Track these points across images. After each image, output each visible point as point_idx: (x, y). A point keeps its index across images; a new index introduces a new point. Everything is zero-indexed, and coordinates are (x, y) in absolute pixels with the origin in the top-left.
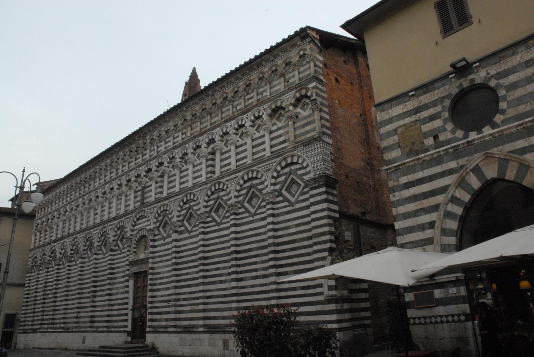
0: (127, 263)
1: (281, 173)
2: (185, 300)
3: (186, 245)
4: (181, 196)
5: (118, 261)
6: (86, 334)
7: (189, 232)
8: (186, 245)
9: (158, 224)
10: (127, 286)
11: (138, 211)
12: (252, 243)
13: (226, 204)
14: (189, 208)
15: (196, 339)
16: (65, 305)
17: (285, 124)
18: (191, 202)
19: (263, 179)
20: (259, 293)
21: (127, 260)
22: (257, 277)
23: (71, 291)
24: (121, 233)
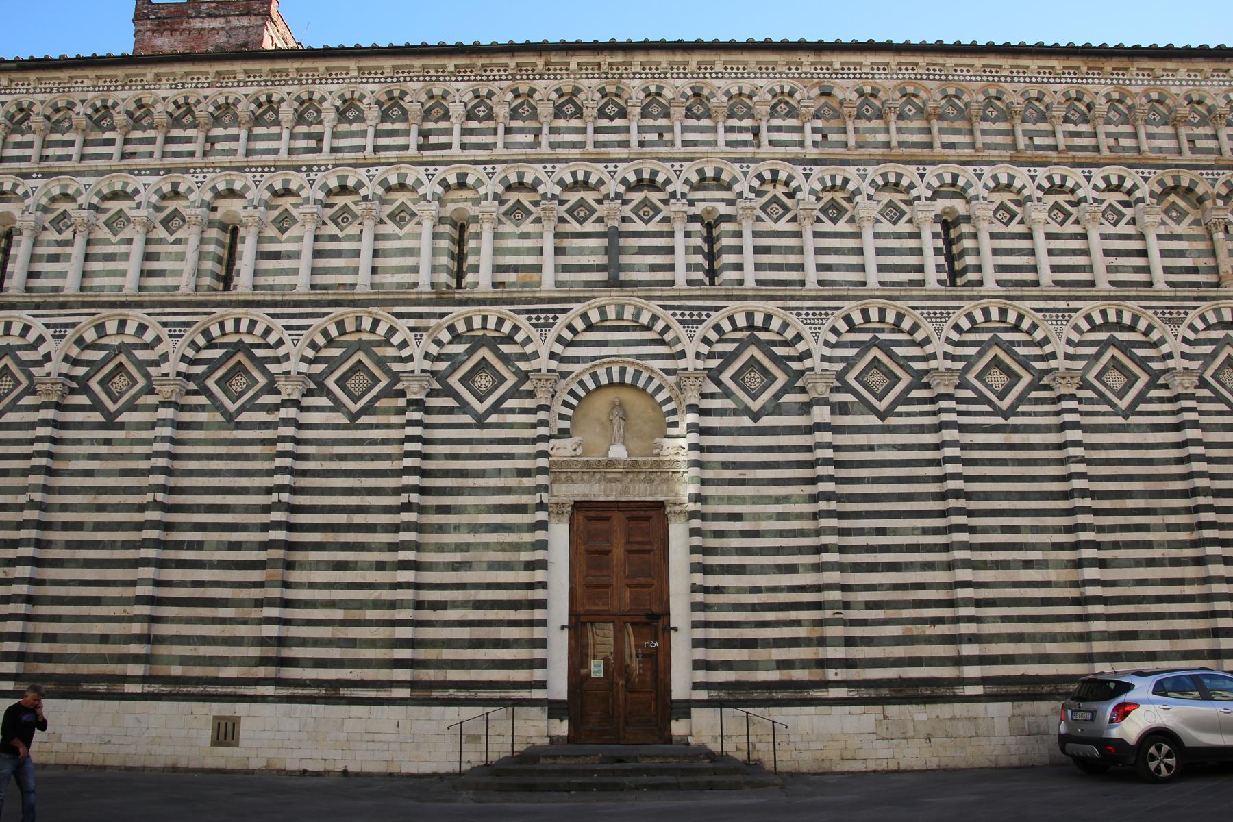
0: (542, 462)
1: (1202, 336)
2: (870, 605)
3: (871, 448)
4: (846, 305)
5: (465, 449)
6: (241, 709)
7: (882, 416)
8: (871, 448)
9: (714, 363)
10: (543, 545)
11: (600, 301)
12: (1130, 478)
13: (1027, 367)
14: (864, 347)
15: (953, 718)
16: (32, 581)
17: (1191, 232)
18: (882, 331)
19: (1155, 336)
20: (1159, 599)
21: (545, 454)
22: (1151, 562)
23: (78, 526)
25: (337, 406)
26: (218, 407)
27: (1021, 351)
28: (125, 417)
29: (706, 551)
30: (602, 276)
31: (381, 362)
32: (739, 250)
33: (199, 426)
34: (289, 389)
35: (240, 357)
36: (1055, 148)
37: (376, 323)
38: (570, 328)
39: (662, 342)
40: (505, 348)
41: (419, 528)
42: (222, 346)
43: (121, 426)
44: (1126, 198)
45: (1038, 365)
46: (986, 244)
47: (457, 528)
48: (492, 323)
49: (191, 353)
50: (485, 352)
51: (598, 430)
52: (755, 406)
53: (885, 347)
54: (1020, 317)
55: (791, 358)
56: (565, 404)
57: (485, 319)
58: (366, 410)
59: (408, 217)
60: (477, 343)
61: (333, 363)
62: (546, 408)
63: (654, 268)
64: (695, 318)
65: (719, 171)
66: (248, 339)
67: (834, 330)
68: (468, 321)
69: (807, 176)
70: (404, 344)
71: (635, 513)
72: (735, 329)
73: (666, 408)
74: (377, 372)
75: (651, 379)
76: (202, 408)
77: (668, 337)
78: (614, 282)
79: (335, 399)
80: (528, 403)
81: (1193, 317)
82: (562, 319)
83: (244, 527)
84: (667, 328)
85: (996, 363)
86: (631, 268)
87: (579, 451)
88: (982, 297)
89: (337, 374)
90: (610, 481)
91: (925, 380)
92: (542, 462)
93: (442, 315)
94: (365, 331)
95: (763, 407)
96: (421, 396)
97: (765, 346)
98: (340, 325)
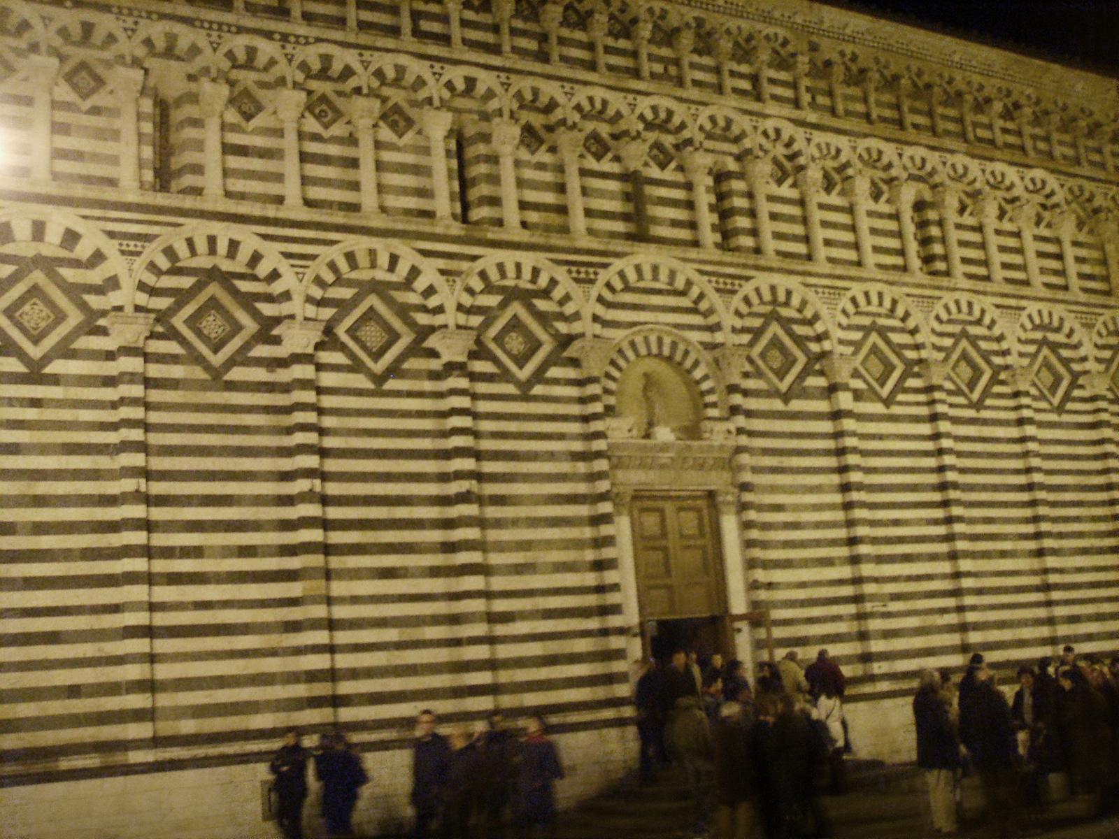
0: (599, 445)
3: (880, 437)
5: (512, 426)
7: (888, 402)
8: (880, 437)
13: (988, 362)
14: (867, 330)
18: (879, 315)
24: (503, 305)
25: (356, 367)
26: (198, 359)
27: (984, 345)
28: (57, 367)
29: (764, 545)
30: (620, 226)
31: (403, 311)
32: (752, 213)
33: (173, 384)
34: (297, 339)
35: (214, 289)
36: (992, 142)
37: (394, 260)
38: (609, 286)
39: (694, 311)
40: (541, 305)
41: (482, 523)
42: (350, 283)
43: (55, 380)
44: (1043, 201)
45: (998, 360)
46: (954, 235)
47: (515, 522)
48: (527, 273)
49: (151, 279)
50: (516, 308)
52: (784, 386)
53: (883, 332)
54: (983, 312)
55: (808, 338)
57: (518, 266)
58: (394, 371)
59: (402, 124)
60: (511, 295)
61: (344, 307)
62: (593, 380)
63: (675, 223)
64: (729, 287)
65: (729, 122)
66: (226, 266)
67: (844, 312)
68: (501, 268)
69: (809, 140)
70: (430, 291)
72: (762, 302)
74: (397, 324)
75: (686, 353)
76: (173, 359)
77: (703, 306)
78: (640, 236)
79: (352, 355)
80: (571, 373)
81: (1099, 326)
82: (603, 276)
83: (255, 526)
84: (702, 296)
85: (964, 356)
86: (655, 221)
88: (955, 289)
89: (348, 322)
91: (916, 369)
92: (599, 445)
93: (474, 258)
94: (381, 268)
95: (789, 389)
96: (462, 358)
97: (786, 323)
98: (350, 257)
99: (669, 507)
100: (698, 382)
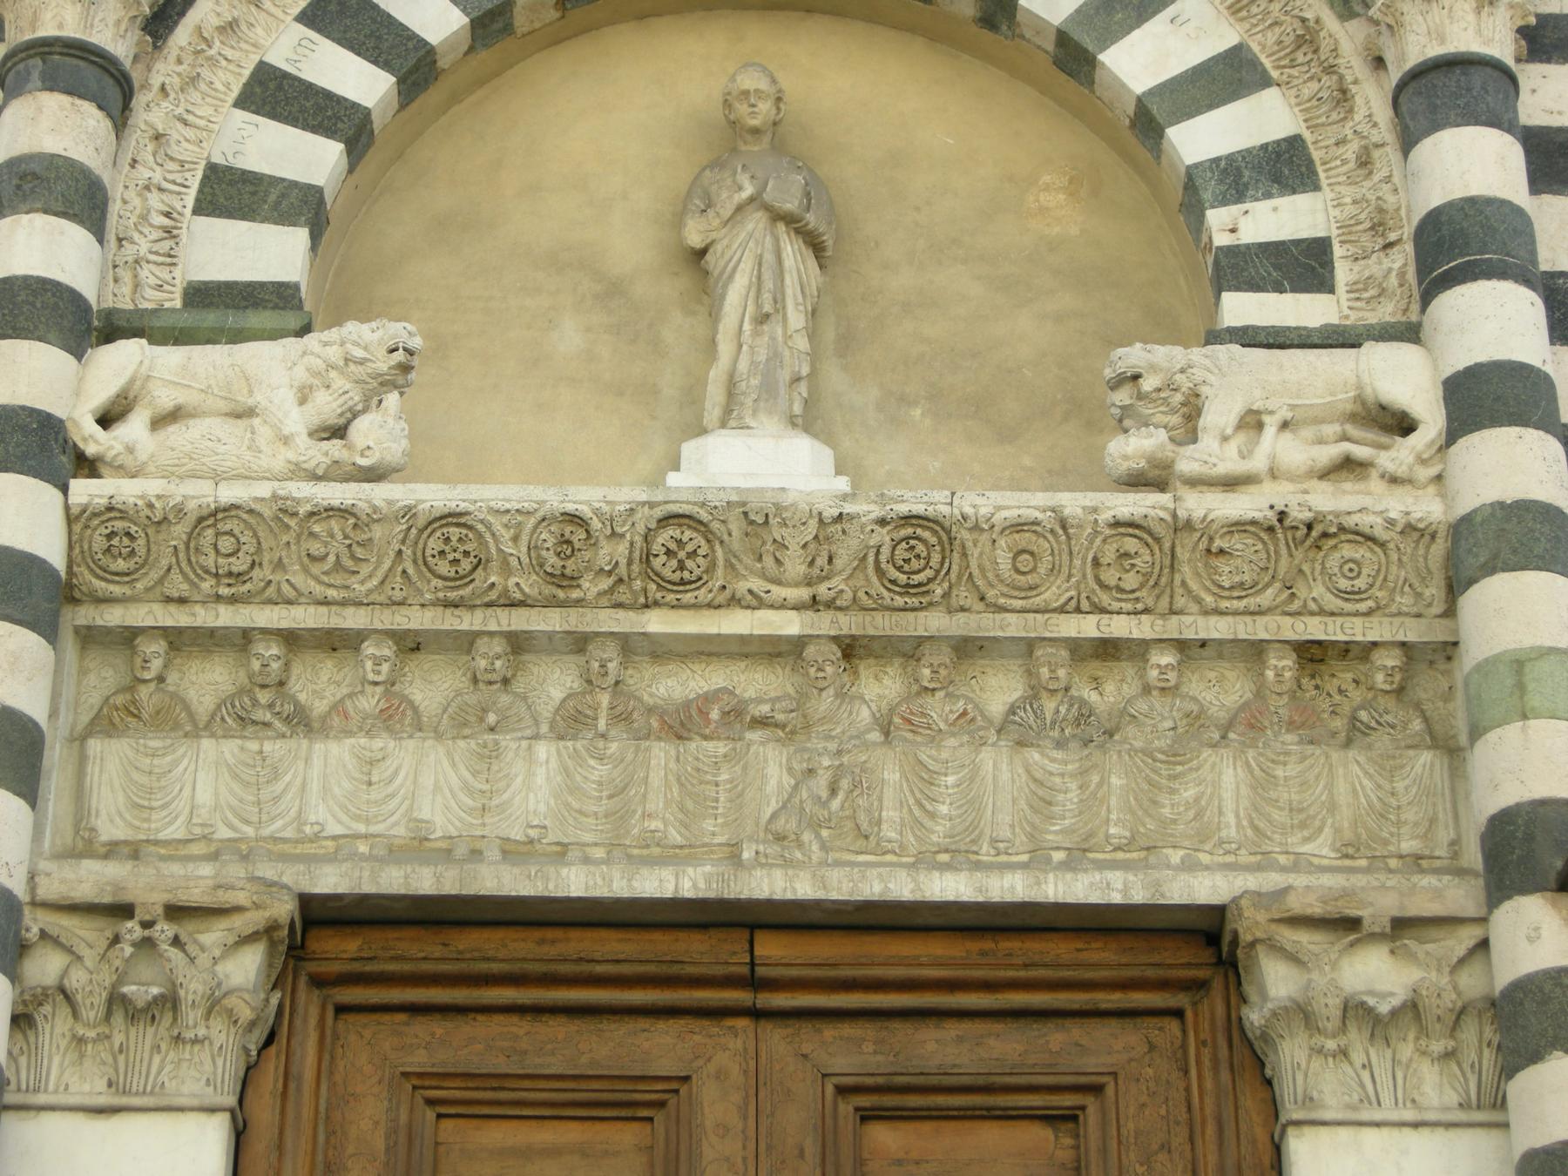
51: (569, 337)
56: (274, 94)
71: (941, 1050)
73: (1200, 139)
87: (379, 434)
90: (681, 724)
99: (718, 1065)
100: (1146, 123)
